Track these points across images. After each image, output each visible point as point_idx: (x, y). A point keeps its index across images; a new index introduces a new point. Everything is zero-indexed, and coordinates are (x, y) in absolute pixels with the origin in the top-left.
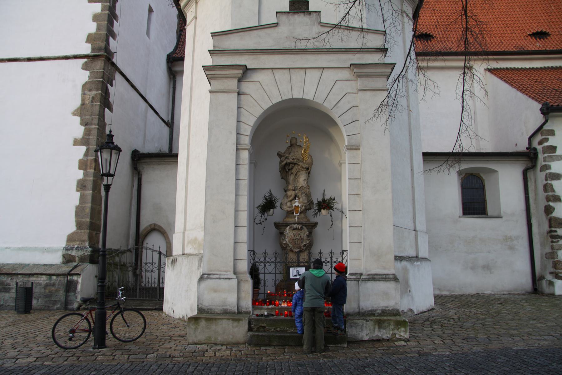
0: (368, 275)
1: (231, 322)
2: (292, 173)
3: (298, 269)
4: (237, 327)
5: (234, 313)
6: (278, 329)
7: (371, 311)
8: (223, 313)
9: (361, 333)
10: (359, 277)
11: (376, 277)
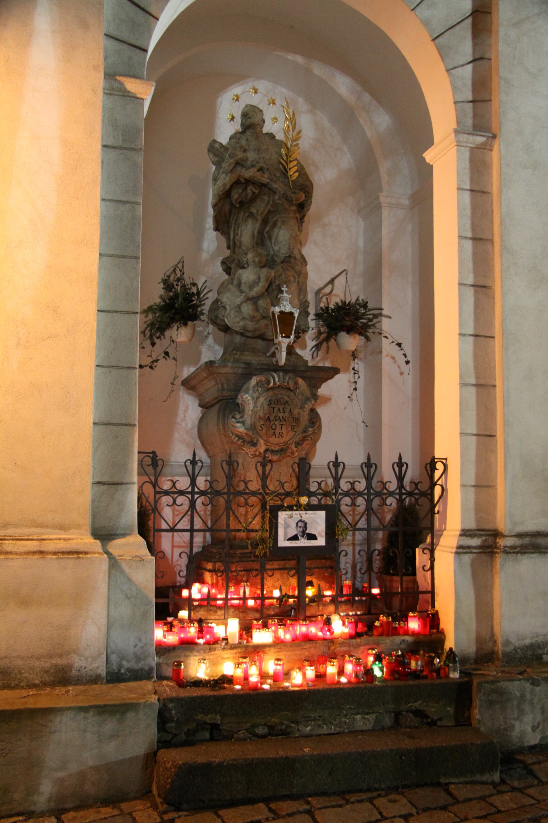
0: (520, 535)
1: (92, 718)
2: (251, 215)
3: (308, 516)
4: (114, 736)
5: (95, 680)
6: (261, 730)
7: (531, 646)
8: (53, 684)
9: (517, 724)
10: (490, 541)
11: (542, 541)
